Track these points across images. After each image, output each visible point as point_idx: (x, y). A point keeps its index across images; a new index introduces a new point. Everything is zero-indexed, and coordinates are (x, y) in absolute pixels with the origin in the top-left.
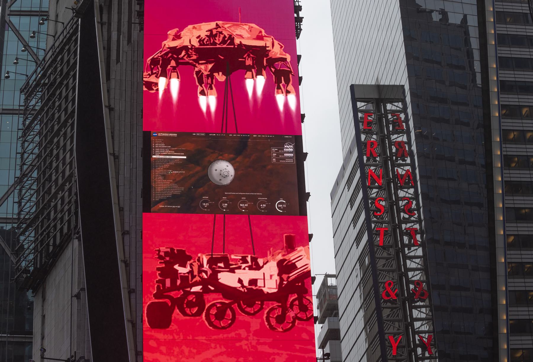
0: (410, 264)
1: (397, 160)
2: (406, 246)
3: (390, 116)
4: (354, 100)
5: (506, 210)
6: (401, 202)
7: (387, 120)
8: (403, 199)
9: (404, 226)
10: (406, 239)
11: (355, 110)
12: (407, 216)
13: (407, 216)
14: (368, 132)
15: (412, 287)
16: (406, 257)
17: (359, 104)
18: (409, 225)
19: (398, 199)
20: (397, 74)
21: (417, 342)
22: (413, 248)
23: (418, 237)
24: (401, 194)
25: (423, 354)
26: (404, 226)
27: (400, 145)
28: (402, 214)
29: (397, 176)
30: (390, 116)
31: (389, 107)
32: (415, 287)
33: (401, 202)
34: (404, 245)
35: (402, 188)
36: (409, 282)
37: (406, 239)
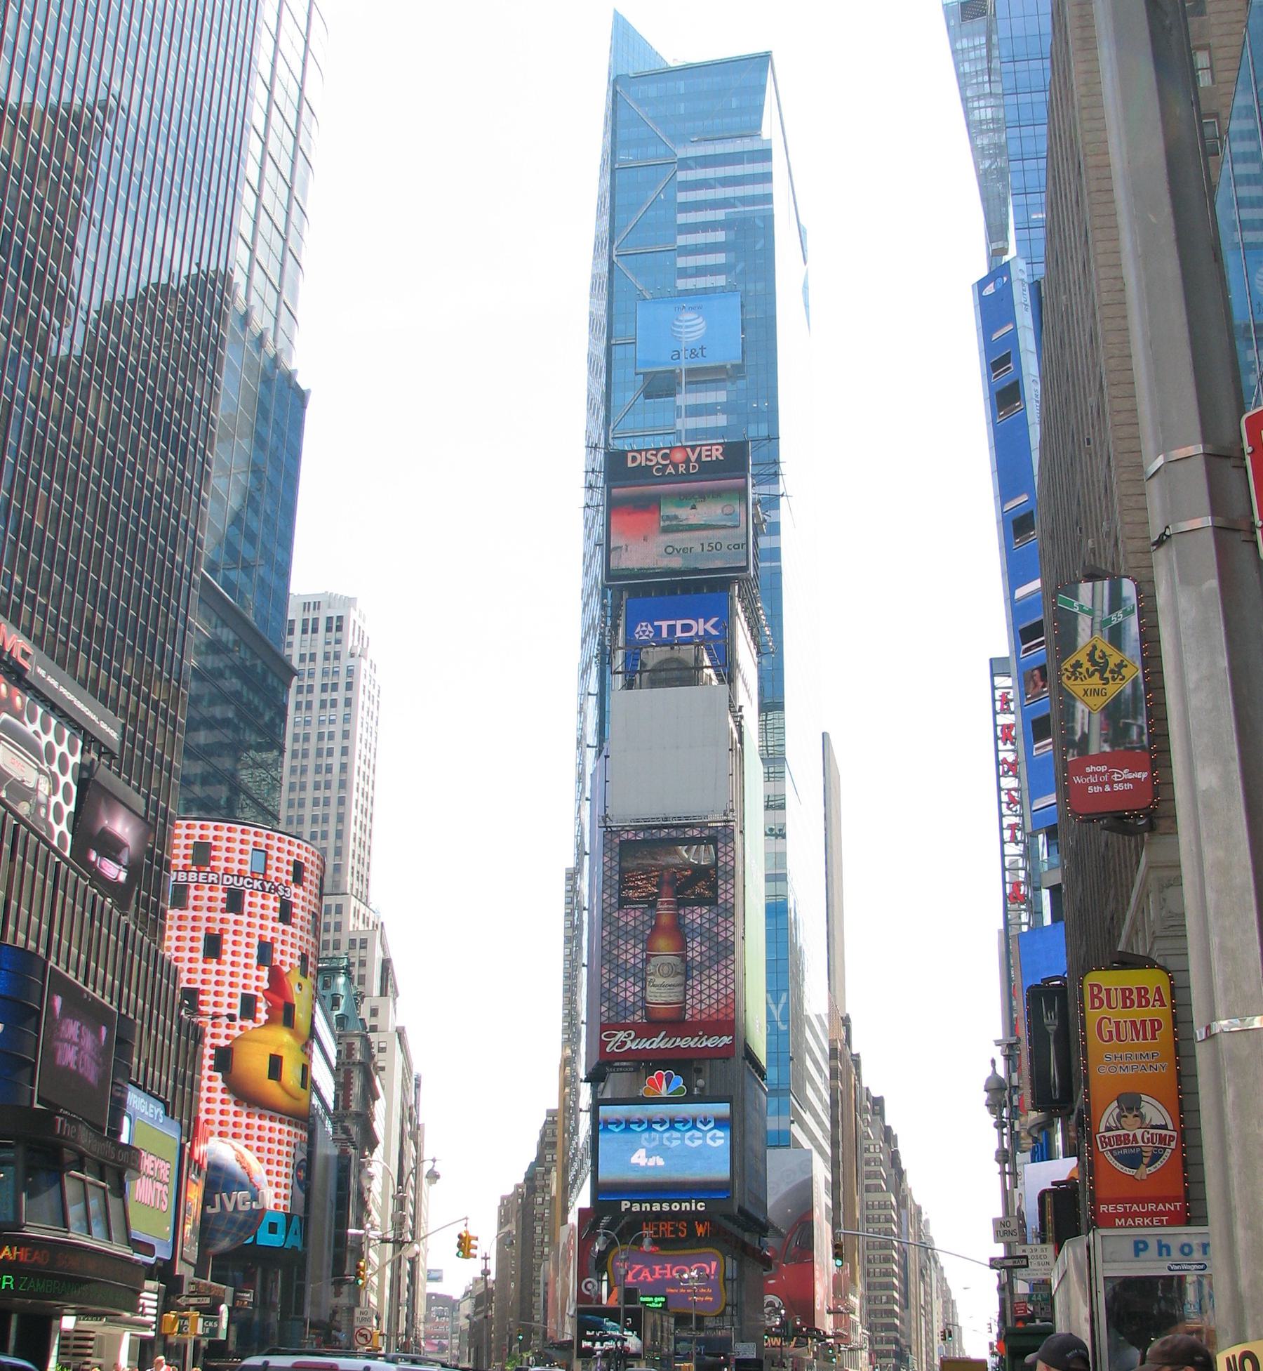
4: (993, 676)
11: (994, 688)
17: (999, 681)
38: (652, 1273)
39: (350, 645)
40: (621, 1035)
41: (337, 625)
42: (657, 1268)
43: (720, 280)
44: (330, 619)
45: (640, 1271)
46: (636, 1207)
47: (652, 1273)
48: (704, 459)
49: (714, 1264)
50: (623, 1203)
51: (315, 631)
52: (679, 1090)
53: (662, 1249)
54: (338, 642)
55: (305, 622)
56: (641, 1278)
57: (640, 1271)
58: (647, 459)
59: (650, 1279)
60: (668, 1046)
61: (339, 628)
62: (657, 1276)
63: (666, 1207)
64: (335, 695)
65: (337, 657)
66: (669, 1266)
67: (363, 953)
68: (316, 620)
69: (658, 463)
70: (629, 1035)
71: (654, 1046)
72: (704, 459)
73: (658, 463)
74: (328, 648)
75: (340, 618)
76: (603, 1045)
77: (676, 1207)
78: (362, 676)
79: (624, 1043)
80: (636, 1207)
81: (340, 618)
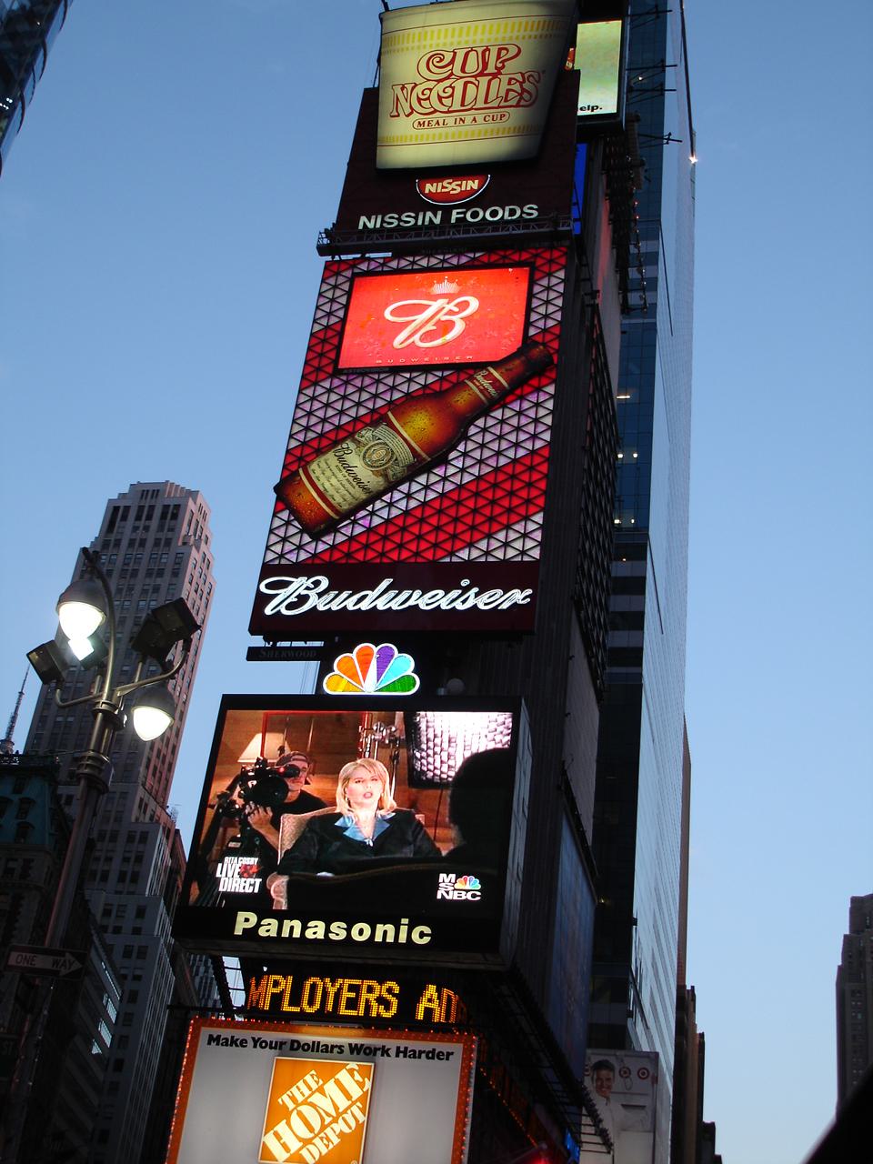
39: (183, 532)
40: (299, 584)
41: (173, 513)
44: (166, 507)
50: (241, 916)
51: (149, 517)
52: (404, 681)
54: (171, 530)
55: (141, 508)
60: (395, 606)
61: (175, 517)
63: (338, 931)
64: (159, 581)
65: (168, 542)
67: (141, 848)
68: (152, 508)
70: (317, 584)
71: (365, 606)
74: (160, 535)
75: (177, 507)
76: (261, 600)
77: (361, 932)
78: (191, 566)
79: (303, 599)
81: (177, 507)
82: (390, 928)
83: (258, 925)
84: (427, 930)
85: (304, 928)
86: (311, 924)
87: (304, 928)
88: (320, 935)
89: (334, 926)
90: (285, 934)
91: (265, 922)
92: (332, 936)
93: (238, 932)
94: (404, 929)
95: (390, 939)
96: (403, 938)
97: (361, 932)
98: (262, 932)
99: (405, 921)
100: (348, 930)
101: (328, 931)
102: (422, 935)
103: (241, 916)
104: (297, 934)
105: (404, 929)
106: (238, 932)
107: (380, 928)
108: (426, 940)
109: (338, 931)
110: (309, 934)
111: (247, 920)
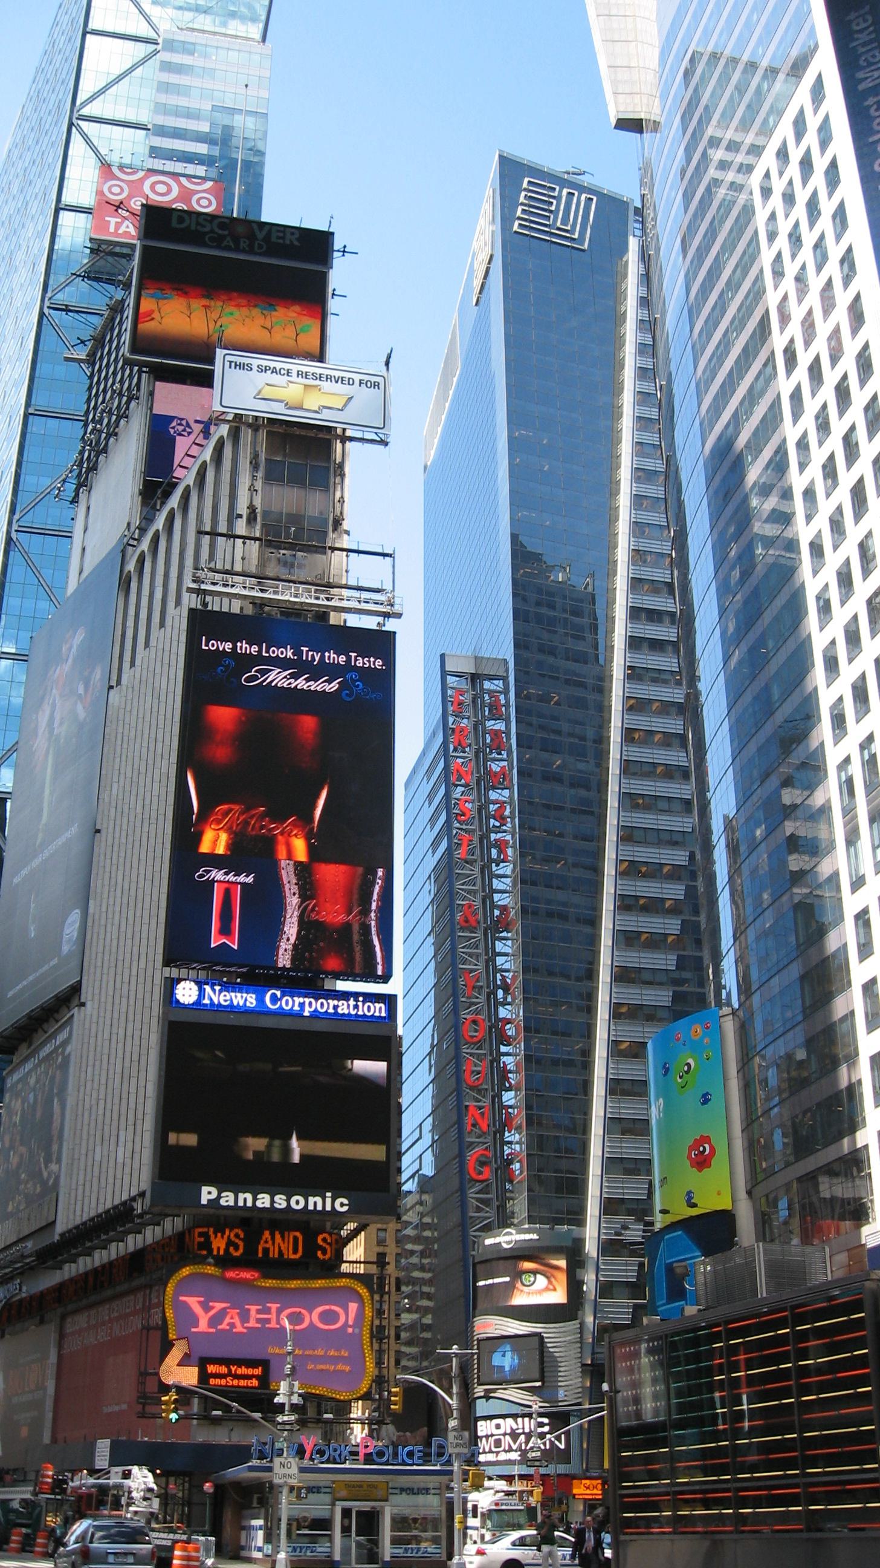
0: (497, 884)
1: (491, 752)
2: (493, 861)
3: (487, 697)
4: (444, 673)
5: (621, 828)
6: (491, 806)
7: (483, 701)
8: (495, 802)
9: (493, 836)
10: (494, 852)
12: (498, 824)
13: (498, 824)
14: (458, 715)
15: (497, 912)
16: (493, 875)
17: (450, 680)
18: (499, 835)
19: (490, 802)
20: (502, 646)
21: (499, 983)
22: (502, 865)
23: (510, 851)
24: (493, 795)
25: (505, 998)
26: (493, 836)
27: (496, 734)
28: (492, 821)
29: (489, 773)
30: (487, 697)
31: (487, 685)
32: (501, 913)
33: (491, 806)
34: (492, 861)
35: (494, 788)
36: (493, 906)
37: (494, 852)
38: (245, 1317)
42: (253, 1309)
43: (201, 170)
45: (223, 1313)
46: (228, 1199)
47: (245, 1317)
48: (274, 239)
49: (353, 1307)
50: (205, 1190)
53: (266, 1276)
56: (224, 1326)
57: (223, 1313)
58: (198, 224)
59: (239, 1329)
62: (252, 1323)
63: (280, 1201)
66: (274, 1307)
69: (212, 231)
72: (274, 239)
73: (212, 231)
77: (298, 1202)
80: (228, 1199)
82: (319, 1200)
83: (219, 1197)
84: (346, 1201)
85: (255, 1199)
86: (259, 1196)
87: (255, 1199)
88: (267, 1205)
89: (277, 1198)
90: (241, 1203)
91: (223, 1194)
92: (276, 1205)
93: (204, 1201)
94: (329, 1201)
95: (319, 1208)
96: (328, 1208)
97: (297, 1202)
98: (223, 1202)
99: (329, 1194)
100: (288, 1201)
101: (272, 1202)
102: (342, 1205)
103: (205, 1190)
104: (249, 1204)
105: (329, 1201)
106: (204, 1201)
107: (311, 1200)
108: (345, 1208)
109: (280, 1201)
110: (259, 1204)
111: (210, 1193)
